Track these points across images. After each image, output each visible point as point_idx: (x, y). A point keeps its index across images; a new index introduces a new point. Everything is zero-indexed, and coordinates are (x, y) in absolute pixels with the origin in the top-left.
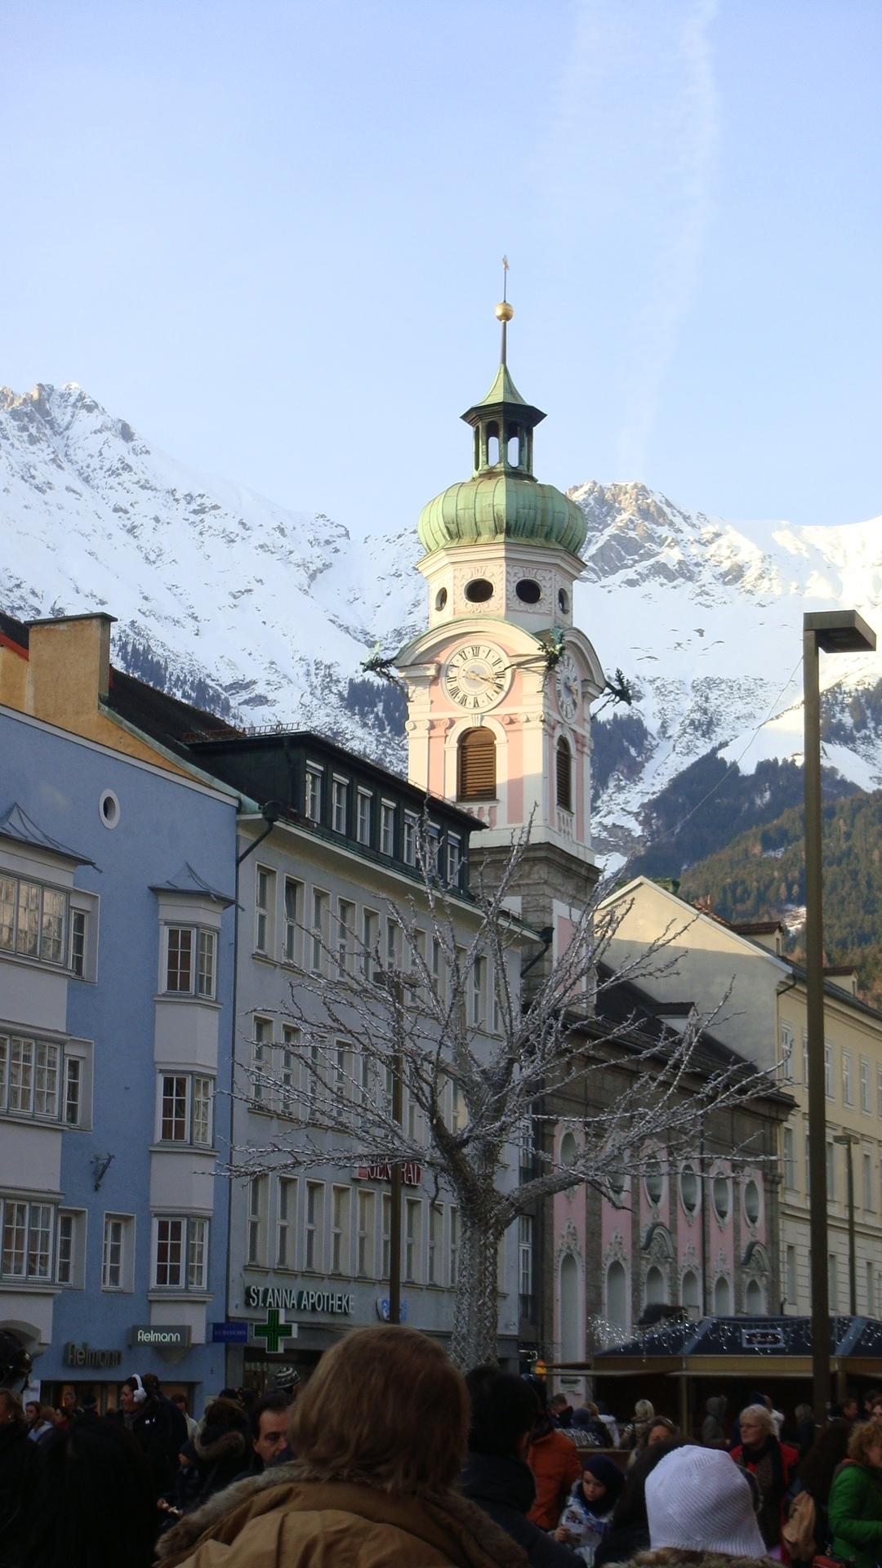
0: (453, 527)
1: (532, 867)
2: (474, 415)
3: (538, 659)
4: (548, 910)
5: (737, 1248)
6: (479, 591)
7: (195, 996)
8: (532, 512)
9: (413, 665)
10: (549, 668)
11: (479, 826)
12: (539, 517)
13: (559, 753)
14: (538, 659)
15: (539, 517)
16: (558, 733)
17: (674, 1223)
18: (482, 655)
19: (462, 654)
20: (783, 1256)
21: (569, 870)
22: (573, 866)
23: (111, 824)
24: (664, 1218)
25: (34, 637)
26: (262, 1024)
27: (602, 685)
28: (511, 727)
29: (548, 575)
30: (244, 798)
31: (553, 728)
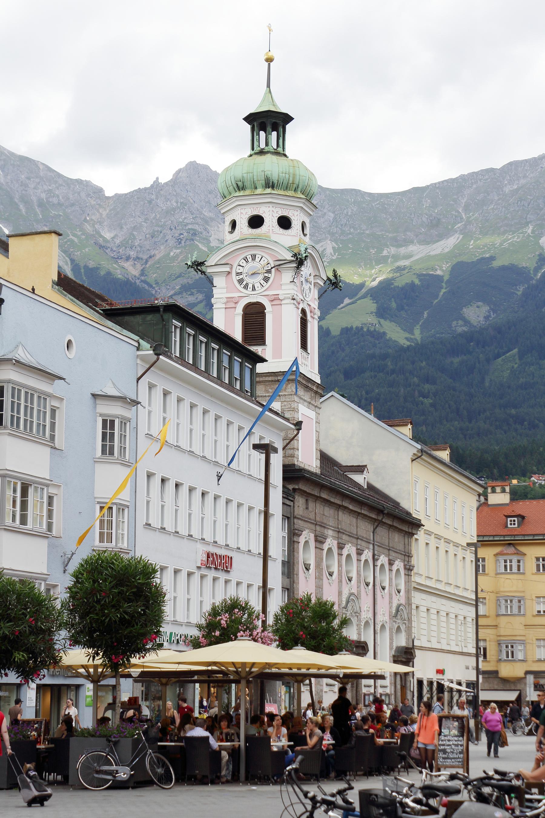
0: (240, 184)
1: (287, 385)
2: (250, 119)
3: (291, 262)
4: (295, 410)
5: (391, 607)
6: (256, 222)
7: (118, 459)
8: (287, 176)
10: (298, 268)
11: (263, 360)
12: (291, 179)
13: (301, 318)
14: (291, 262)
15: (291, 179)
16: (301, 307)
17: (359, 592)
18: (257, 260)
19: (246, 259)
20: (414, 612)
21: (307, 387)
22: (310, 385)
23: (72, 354)
24: (354, 591)
25: (13, 243)
26: (150, 476)
27: (325, 279)
29: (296, 213)
30: (141, 341)
31: (299, 304)
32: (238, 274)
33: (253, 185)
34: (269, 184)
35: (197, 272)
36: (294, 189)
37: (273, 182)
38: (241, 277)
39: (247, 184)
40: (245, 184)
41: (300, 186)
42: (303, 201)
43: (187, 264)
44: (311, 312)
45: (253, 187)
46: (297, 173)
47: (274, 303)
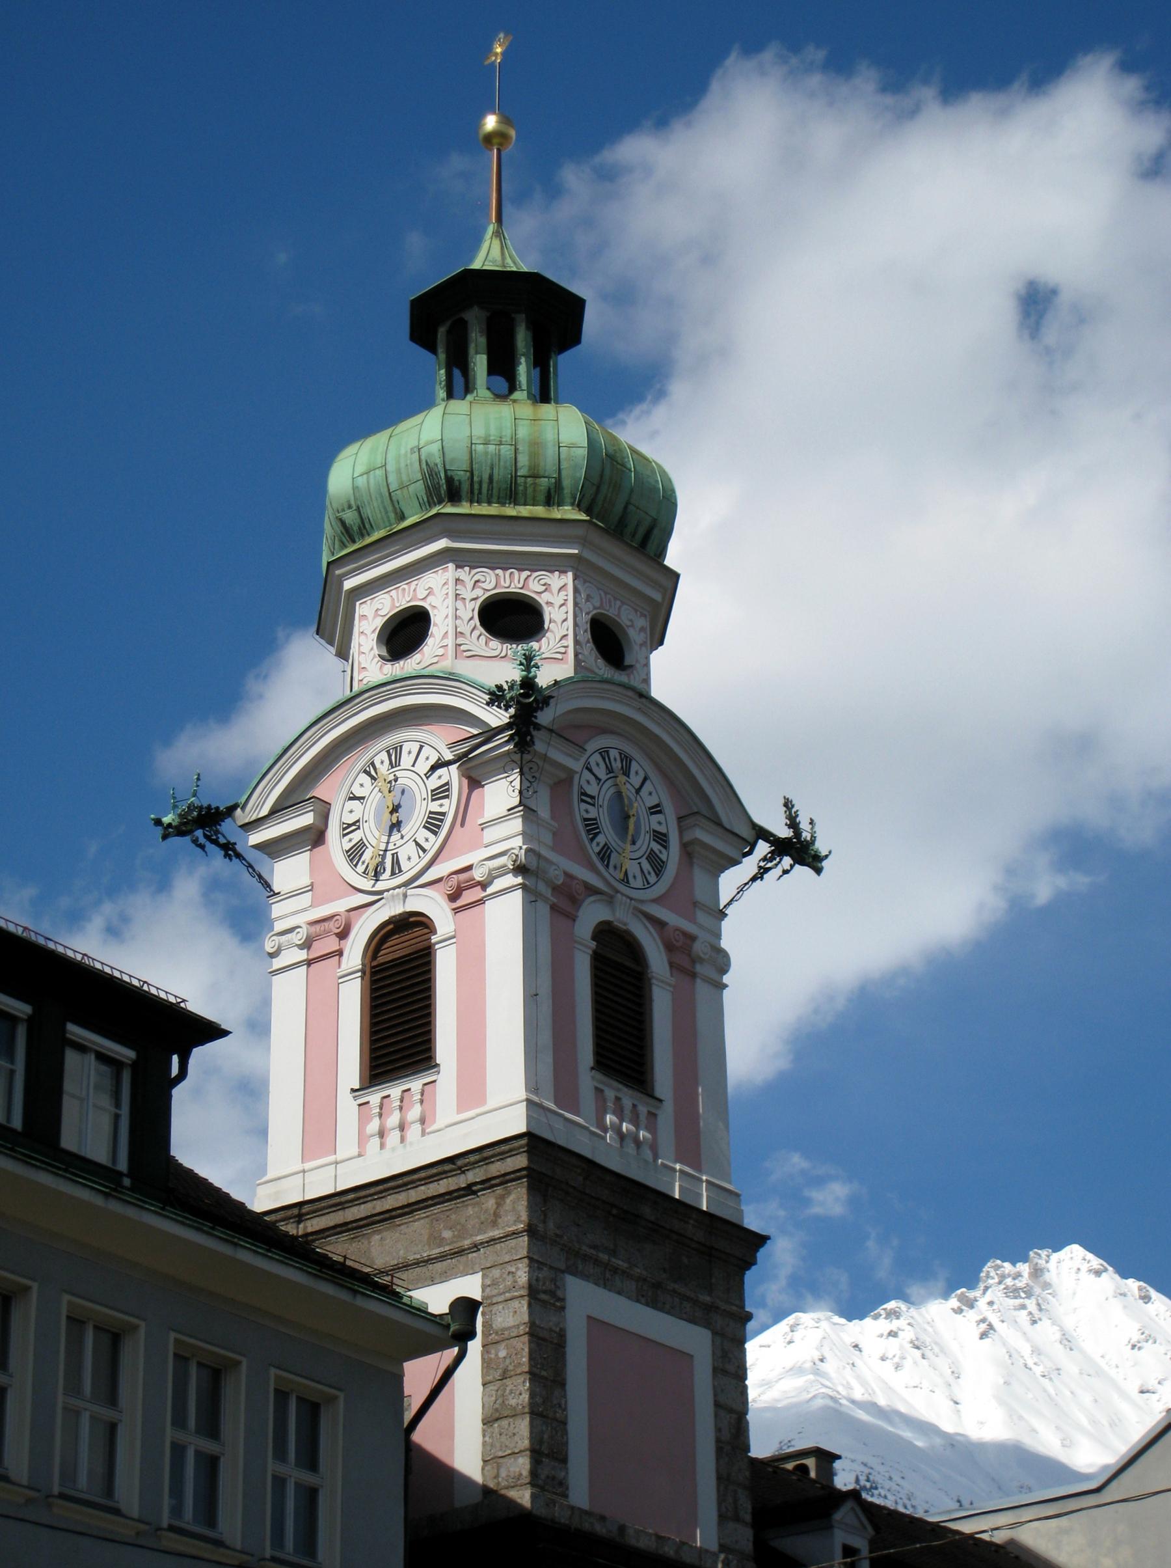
0: (350, 517)
8: (507, 451)
9: (274, 812)
15: (523, 460)
16: (592, 915)
18: (406, 760)
19: (370, 771)
22: (647, 1211)
27: (746, 833)
28: (468, 897)
31: (576, 902)
32: (348, 828)
33: (390, 508)
34: (437, 488)
35: (202, 847)
36: (541, 497)
37: (450, 480)
38: (356, 836)
39: (373, 511)
40: (368, 512)
41: (566, 483)
42: (580, 531)
43: (158, 822)
44: (670, 947)
45: (392, 515)
46: (549, 435)
47: (459, 903)
